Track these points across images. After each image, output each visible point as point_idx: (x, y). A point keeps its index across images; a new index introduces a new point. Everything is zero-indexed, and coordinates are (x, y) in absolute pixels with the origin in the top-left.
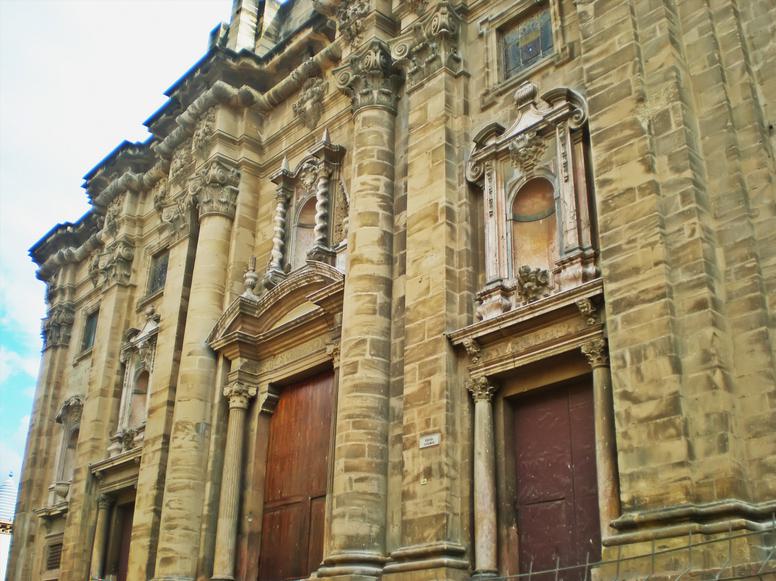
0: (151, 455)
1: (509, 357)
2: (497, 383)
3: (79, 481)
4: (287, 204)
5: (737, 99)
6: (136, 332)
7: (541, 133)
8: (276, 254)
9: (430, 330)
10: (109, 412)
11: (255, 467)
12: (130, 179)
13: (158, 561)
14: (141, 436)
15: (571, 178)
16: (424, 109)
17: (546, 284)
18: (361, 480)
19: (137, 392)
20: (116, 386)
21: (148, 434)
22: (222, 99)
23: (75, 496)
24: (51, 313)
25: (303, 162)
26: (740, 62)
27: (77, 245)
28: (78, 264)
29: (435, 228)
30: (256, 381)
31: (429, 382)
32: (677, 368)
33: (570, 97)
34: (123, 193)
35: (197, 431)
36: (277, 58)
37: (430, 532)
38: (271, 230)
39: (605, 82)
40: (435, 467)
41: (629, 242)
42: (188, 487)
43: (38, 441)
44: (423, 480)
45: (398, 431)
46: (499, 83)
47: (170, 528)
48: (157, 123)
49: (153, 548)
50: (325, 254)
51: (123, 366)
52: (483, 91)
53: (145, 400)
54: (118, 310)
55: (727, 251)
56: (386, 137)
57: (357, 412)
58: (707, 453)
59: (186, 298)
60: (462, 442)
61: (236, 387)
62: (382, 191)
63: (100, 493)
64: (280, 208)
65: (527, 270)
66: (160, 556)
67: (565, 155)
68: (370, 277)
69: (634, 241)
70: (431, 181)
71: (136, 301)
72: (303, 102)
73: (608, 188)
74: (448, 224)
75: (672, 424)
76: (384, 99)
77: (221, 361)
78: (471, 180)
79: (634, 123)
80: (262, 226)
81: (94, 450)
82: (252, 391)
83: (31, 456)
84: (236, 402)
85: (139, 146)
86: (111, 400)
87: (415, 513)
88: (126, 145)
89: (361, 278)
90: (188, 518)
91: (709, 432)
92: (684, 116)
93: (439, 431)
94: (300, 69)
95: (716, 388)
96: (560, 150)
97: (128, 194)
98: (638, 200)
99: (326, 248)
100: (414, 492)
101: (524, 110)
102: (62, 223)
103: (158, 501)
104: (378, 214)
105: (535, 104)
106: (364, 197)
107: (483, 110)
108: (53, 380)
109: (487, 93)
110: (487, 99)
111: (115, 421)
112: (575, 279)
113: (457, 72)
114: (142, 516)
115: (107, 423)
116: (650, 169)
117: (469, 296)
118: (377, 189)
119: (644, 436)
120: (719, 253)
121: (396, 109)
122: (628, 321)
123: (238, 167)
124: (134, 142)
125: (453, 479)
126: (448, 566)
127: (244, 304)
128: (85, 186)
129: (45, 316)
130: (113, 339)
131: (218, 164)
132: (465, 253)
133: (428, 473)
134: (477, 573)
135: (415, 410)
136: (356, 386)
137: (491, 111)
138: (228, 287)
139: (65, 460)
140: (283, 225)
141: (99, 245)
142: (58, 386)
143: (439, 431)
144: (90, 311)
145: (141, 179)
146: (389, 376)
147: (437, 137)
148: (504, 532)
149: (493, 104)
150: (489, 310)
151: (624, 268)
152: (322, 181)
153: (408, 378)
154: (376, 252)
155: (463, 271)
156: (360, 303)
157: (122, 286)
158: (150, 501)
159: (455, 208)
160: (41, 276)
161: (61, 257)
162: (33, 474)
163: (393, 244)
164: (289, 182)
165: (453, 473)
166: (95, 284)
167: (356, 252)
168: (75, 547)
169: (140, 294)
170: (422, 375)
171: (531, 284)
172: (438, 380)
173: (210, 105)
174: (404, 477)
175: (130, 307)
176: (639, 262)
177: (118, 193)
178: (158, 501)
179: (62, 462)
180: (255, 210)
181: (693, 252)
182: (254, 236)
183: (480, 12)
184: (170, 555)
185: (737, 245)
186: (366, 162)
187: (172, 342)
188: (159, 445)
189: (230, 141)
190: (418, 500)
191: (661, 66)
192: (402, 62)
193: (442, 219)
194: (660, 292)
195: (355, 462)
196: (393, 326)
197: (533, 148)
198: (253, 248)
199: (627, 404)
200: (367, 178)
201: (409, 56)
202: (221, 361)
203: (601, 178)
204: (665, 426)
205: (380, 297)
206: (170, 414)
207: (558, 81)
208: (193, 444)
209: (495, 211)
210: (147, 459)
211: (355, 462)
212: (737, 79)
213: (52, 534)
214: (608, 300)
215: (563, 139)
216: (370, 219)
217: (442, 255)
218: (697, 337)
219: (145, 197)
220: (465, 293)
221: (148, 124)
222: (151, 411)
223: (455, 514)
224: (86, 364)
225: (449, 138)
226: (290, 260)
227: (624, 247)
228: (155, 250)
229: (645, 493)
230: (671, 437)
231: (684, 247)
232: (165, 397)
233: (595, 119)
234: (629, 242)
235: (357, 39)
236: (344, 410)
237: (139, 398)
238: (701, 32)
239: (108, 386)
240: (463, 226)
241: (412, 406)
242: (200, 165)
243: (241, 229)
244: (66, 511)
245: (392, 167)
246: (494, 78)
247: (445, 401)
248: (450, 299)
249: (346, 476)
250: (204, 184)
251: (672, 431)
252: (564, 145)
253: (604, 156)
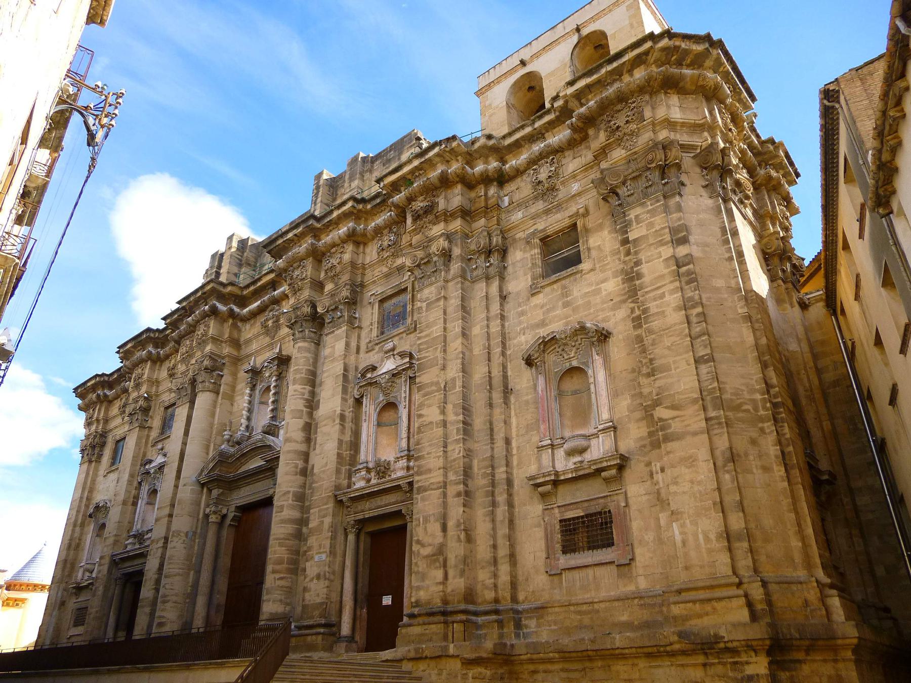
0: (155, 550)
1: (369, 509)
2: (362, 523)
3: (103, 565)
4: (253, 388)
5: (496, 372)
6: (150, 462)
7: (394, 375)
8: (244, 422)
9: (326, 490)
10: (128, 516)
11: (226, 561)
12: (150, 353)
13: (155, 625)
14: (149, 535)
15: (407, 406)
16: (333, 347)
17: (389, 468)
18: (281, 578)
19: (148, 503)
20: (134, 497)
21: (154, 535)
22: (214, 312)
23: (100, 575)
24: (87, 437)
25: (264, 361)
26: (499, 350)
27: (111, 387)
28: (110, 402)
29: (333, 426)
30: (227, 504)
31: (322, 522)
32: (444, 529)
33: (411, 356)
34: (147, 361)
35: (187, 537)
36: (252, 288)
37: (317, 613)
38: (242, 402)
39: (427, 355)
40: (322, 573)
41: (428, 454)
42: (179, 574)
43: (73, 531)
44: (315, 581)
45: (305, 548)
46: (377, 336)
47: (164, 602)
48: (174, 319)
49: (152, 614)
50: (271, 430)
51: (140, 483)
52: (368, 340)
53: (154, 508)
54: (138, 444)
55: (478, 462)
56: (311, 360)
57: (282, 536)
58: (454, 577)
59: (184, 444)
60: (339, 559)
61: (213, 509)
62: (306, 396)
63: (117, 574)
64: (248, 391)
65: (380, 460)
66: (156, 621)
67: (405, 392)
68: (296, 452)
69: (430, 453)
70: (333, 395)
71: (151, 438)
72: (267, 320)
73: (421, 420)
74: (341, 424)
75: (437, 560)
76: (312, 335)
77: (205, 490)
78: (357, 397)
79: (438, 383)
80: (237, 398)
81: (116, 542)
82: (224, 511)
83: (67, 542)
84: (213, 518)
85: (158, 330)
86: (130, 508)
87: (310, 601)
88: (149, 330)
89: (289, 452)
90: (176, 595)
91: (456, 566)
92: (463, 382)
93: (326, 552)
94: (266, 298)
95: (461, 542)
96: (403, 389)
97: (149, 362)
98: (435, 430)
99: (274, 423)
100: (310, 589)
101: (388, 358)
103: (158, 582)
104: (303, 411)
105: (394, 355)
106: (295, 399)
107: (367, 352)
108: (87, 488)
109: (370, 341)
110: (370, 345)
111: (131, 523)
112: (403, 469)
113: (353, 324)
114: (146, 592)
115: (126, 523)
116: (443, 412)
117: (350, 470)
119: (425, 566)
120: (475, 463)
121: (319, 341)
122: (423, 499)
123: (223, 358)
124: (155, 328)
125: (332, 581)
126: (323, 634)
127: (222, 454)
128: (118, 352)
129: (83, 438)
130: (133, 465)
131: (210, 356)
132: (349, 443)
133: (318, 577)
134: (340, 638)
135: (315, 537)
136: (282, 520)
137: (371, 354)
138: (213, 440)
139: (93, 544)
140: (250, 402)
141: (125, 391)
142: (91, 491)
143: (326, 552)
144: (118, 438)
145: (158, 353)
146: (302, 513)
147: (339, 368)
148: (358, 613)
149: (373, 350)
150: (359, 480)
151: (424, 468)
152: (274, 378)
153: (312, 518)
154: (299, 435)
155: (346, 453)
156: (288, 468)
157: (142, 427)
158: (153, 582)
159: (347, 414)
160: (80, 408)
161: (98, 395)
162: (67, 555)
163: (309, 429)
164: (255, 373)
165: (332, 577)
166: (123, 419)
167: (288, 435)
168: (97, 612)
169: (154, 434)
170: (320, 517)
171: (382, 469)
172: (328, 520)
173: (205, 315)
174: (305, 578)
175: (147, 443)
176: (431, 466)
177: (142, 361)
178: (158, 582)
179: (91, 546)
180: (233, 388)
181: (458, 464)
182: (232, 405)
183: (371, 287)
184: (164, 620)
185: (484, 460)
186: (298, 376)
187: (174, 474)
188: (161, 544)
190: (312, 593)
191: (455, 350)
192: (322, 314)
193: (338, 421)
194: (439, 485)
195: (278, 567)
196: (307, 482)
197: (390, 384)
198: (231, 413)
199: (419, 546)
200: (298, 387)
201: (327, 311)
202: (205, 490)
203: (419, 413)
204: (435, 561)
205: (301, 464)
206: (170, 523)
207: (405, 344)
208: (183, 545)
209: (367, 419)
210: (152, 552)
211: (278, 567)
212: (497, 359)
213: (79, 600)
214: (416, 486)
215: (406, 380)
216: (298, 414)
217: (336, 444)
218: (456, 511)
219: (161, 366)
220: (347, 467)
221: (164, 319)
222: (157, 520)
223: (331, 602)
224: (113, 476)
225: (346, 370)
226: (253, 423)
227: (426, 456)
228: (167, 404)
229: (422, 598)
230: (436, 568)
231: (454, 460)
232: (167, 511)
233: (419, 376)
234: (428, 454)
235: (298, 294)
236: (274, 534)
237: (150, 507)
238: (481, 329)
239: (129, 497)
240: (349, 425)
241: (313, 535)
242: (198, 354)
243: (224, 400)
244: (91, 584)
245: (313, 380)
246: (375, 333)
247: (330, 534)
248: (338, 471)
249: (273, 576)
250: (200, 370)
251: (438, 564)
252: (405, 385)
253: (422, 399)
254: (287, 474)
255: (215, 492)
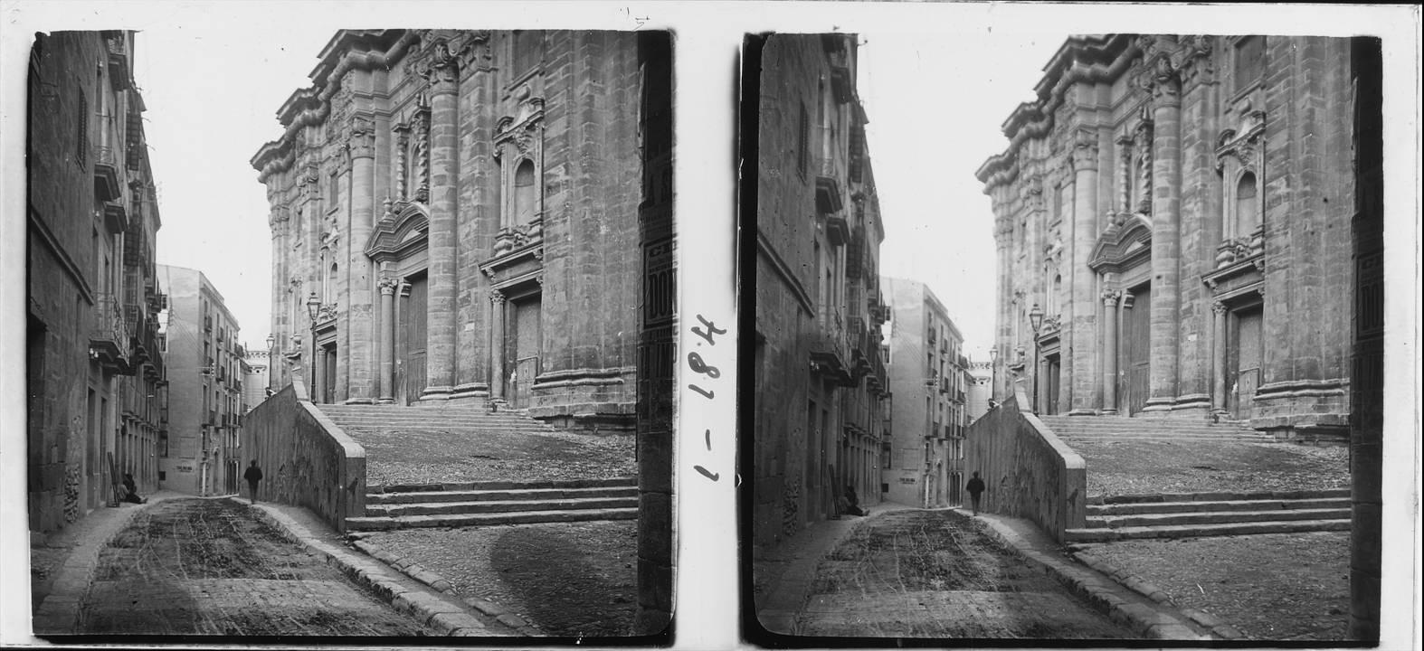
72: (1132, 78)
77: (1098, 275)
102: (993, 155)
107: (1226, 112)
118: (1167, 169)
169: (1050, 217)
177: (1025, 140)
188: (1068, 330)
189: (1088, 110)
202: (1098, 275)
254: (1159, 257)
255: (1107, 277)
